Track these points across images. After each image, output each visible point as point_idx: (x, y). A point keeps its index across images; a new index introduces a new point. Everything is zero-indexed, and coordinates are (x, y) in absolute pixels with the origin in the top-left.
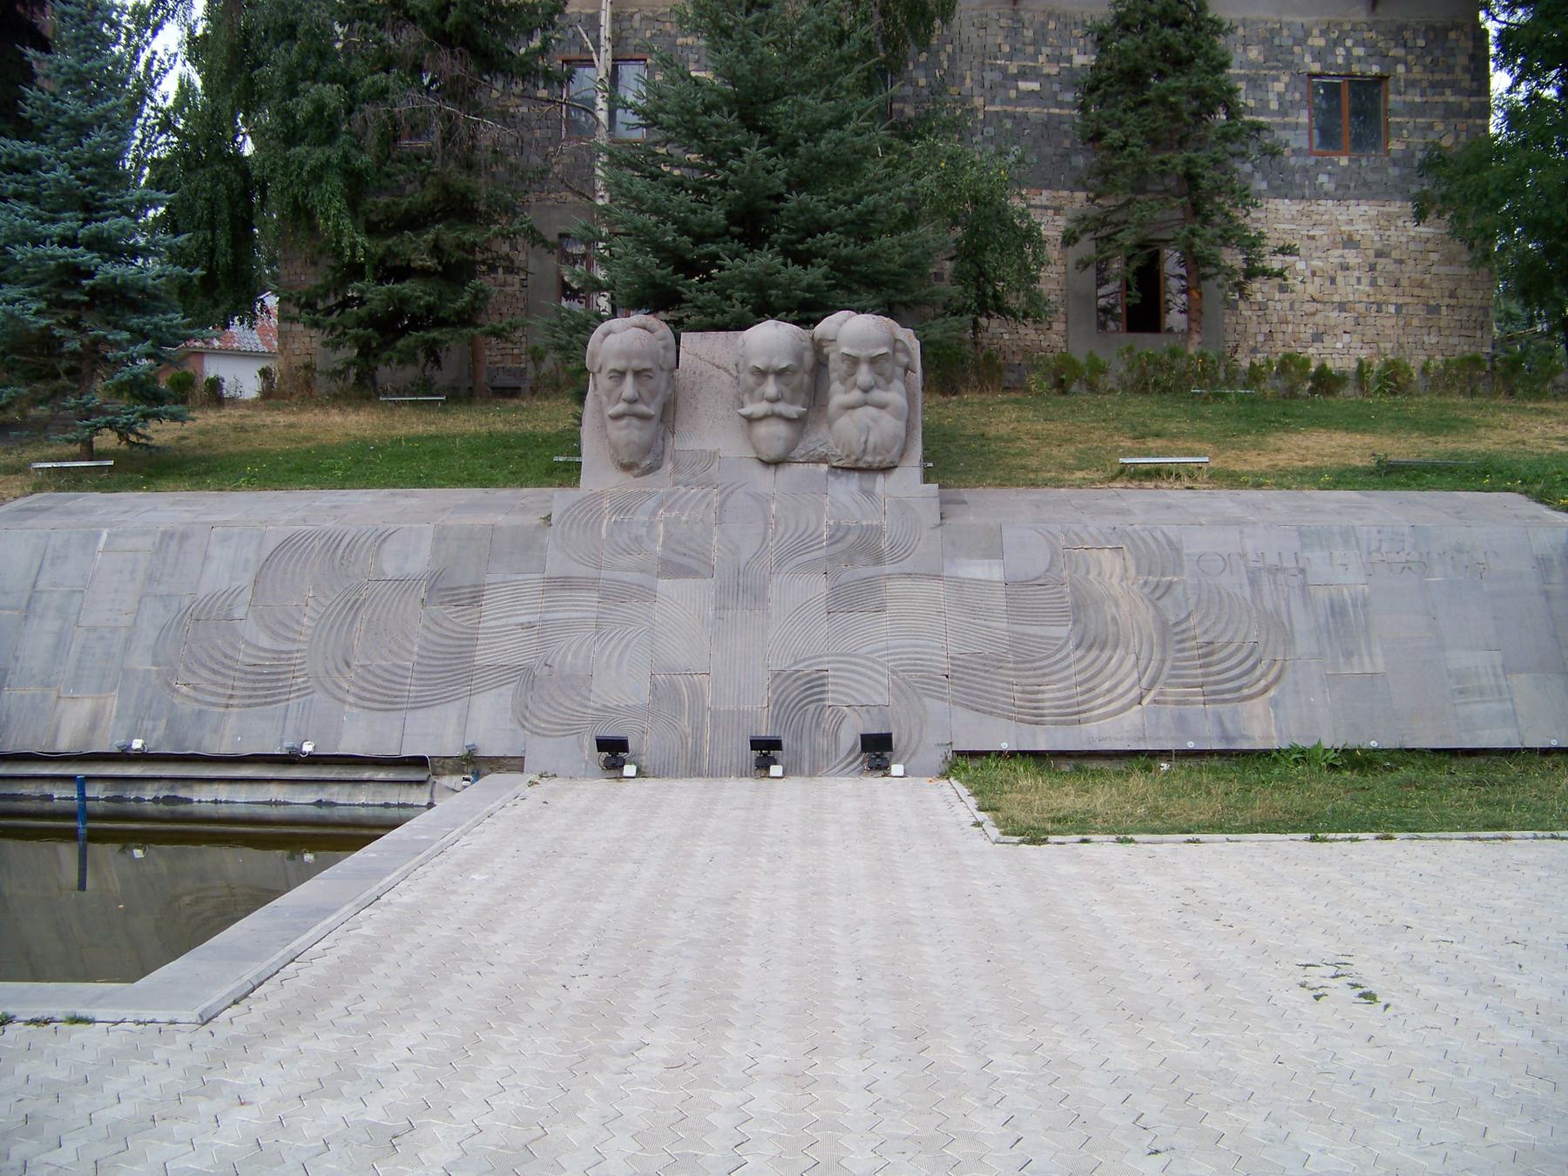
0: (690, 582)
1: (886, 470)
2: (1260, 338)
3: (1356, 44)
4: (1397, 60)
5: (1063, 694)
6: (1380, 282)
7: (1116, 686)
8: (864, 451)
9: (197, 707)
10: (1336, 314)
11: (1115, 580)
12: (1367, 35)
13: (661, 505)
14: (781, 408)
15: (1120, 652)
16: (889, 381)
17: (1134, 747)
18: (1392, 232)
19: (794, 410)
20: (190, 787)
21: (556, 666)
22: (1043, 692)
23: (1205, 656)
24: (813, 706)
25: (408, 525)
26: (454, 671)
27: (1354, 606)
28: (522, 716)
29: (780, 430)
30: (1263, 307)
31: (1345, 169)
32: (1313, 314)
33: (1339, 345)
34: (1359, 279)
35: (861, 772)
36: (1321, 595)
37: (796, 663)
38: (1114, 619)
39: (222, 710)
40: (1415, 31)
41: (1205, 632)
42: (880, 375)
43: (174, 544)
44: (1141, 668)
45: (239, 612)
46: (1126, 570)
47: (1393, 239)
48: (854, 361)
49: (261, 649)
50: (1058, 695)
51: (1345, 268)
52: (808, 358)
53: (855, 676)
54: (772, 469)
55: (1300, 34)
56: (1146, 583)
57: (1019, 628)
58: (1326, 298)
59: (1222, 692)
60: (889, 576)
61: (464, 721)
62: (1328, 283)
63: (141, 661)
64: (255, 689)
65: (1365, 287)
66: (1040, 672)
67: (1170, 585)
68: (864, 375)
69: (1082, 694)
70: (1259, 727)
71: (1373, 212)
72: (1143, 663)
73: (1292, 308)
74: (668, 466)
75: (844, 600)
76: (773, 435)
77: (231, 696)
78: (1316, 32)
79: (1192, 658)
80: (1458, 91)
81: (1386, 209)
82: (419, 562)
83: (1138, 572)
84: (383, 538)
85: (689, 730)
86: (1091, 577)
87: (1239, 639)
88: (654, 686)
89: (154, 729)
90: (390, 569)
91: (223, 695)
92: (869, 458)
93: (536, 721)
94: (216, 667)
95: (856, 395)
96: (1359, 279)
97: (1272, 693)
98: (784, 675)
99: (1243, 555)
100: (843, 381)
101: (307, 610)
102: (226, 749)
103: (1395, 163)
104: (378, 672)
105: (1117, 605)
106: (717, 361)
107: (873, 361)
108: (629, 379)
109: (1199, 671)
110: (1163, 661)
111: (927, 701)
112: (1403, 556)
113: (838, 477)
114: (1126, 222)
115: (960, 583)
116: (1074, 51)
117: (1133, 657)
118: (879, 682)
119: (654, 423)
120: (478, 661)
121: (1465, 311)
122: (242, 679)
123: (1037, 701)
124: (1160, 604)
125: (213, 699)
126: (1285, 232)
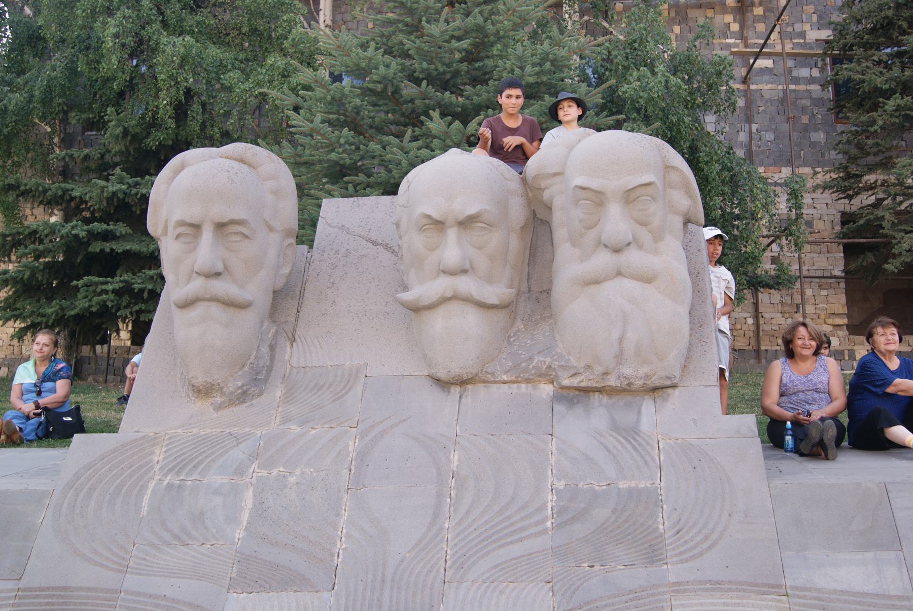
8: (620, 357)
13: (254, 456)
14: (466, 285)
16: (658, 237)
19: (494, 293)
29: (470, 322)
42: (643, 224)
48: (597, 199)
52: (517, 212)
54: (456, 390)
60: (678, 588)
76: (459, 335)
92: (627, 371)
95: (603, 260)
106: (374, 236)
107: (630, 196)
108: (207, 235)
116: (807, 27)
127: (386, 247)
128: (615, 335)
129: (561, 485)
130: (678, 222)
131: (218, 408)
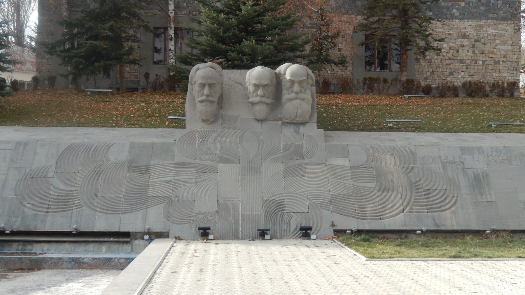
0: (231, 166)
1: (304, 124)
2: (429, 74)
5: (374, 208)
6: (476, 52)
7: (394, 206)
8: (296, 116)
10: (458, 64)
11: (392, 166)
13: (218, 136)
15: (395, 193)
16: (305, 90)
17: (402, 228)
18: (481, 32)
19: (269, 101)
20: (32, 245)
21: (180, 197)
22: (366, 208)
24: (280, 213)
25: (118, 141)
26: (140, 199)
27: (483, 176)
28: (168, 217)
30: (430, 62)
31: (463, 7)
32: (450, 64)
33: (460, 77)
34: (468, 51)
35: (300, 237)
36: (470, 172)
37: (273, 196)
38: (392, 180)
39: (45, 214)
41: (427, 186)
42: (302, 87)
44: (403, 199)
45: (50, 175)
46: (396, 162)
47: (482, 35)
49: (60, 189)
50: (372, 209)
51: (463, 46)
52: (274, 80)
53: (295, 201)
56: (403, 167)
57: (356, 184)
58: (455, 58)
59: (434, 208)
61: (145, 218)
62: (455, 52)
63: (9, 194)
64: (58, 205)
65: (470, 54)
66: (365, 200)
67: (413, 168)
68: (296, 88)
69: (381, 208)
70: (450, 221)
71: (474, 24)
72: (403, 197)
73: (441, 62)
74: (221, 121)
75: (290, 173)
76: (261, 110)
77: (48, 208)
79: (422, 195)
81: (479, 23)
82: (124, 156)
83: (400, 163)
84: (108, 147)
85: (233, 222)
86: (383, 164)
87: (440, 188)
88: (219, 205)
89: (16, 221)
90: (112, 159)
91: (45, 208)
92: (298, 119)
93: (173, 218)
94: (42, 197)
96: (468, 51)
97: (453, 209)
98: (269, 201)
99: (440, 157)
100: (288, 90)
101: (79, 174)
102: (47, 228)
103: (483, 5)
104: (109, 199)
105: (393, 175)
106: (237, 81)
107: (300, 82)
108: (207, 88)
109: (425, 200)
110: (411, 197)
111: (323, 211)
112: (501, 158)
113: (286, 126)
114: (378, 28)
115: (333, 167)
117: (400, 195)
118: (304, 204)
119: (215, 104)
120: (150, 195)
121: (510, 63)
122: (52, 202)
123: (364, 211)
124: (409, 175)
125: (41, 209)
126: (439, 32)
127: (241, 84)
128: (296, 112)
129: (284, 143)
130: (310, 86)
131: (208, 124)
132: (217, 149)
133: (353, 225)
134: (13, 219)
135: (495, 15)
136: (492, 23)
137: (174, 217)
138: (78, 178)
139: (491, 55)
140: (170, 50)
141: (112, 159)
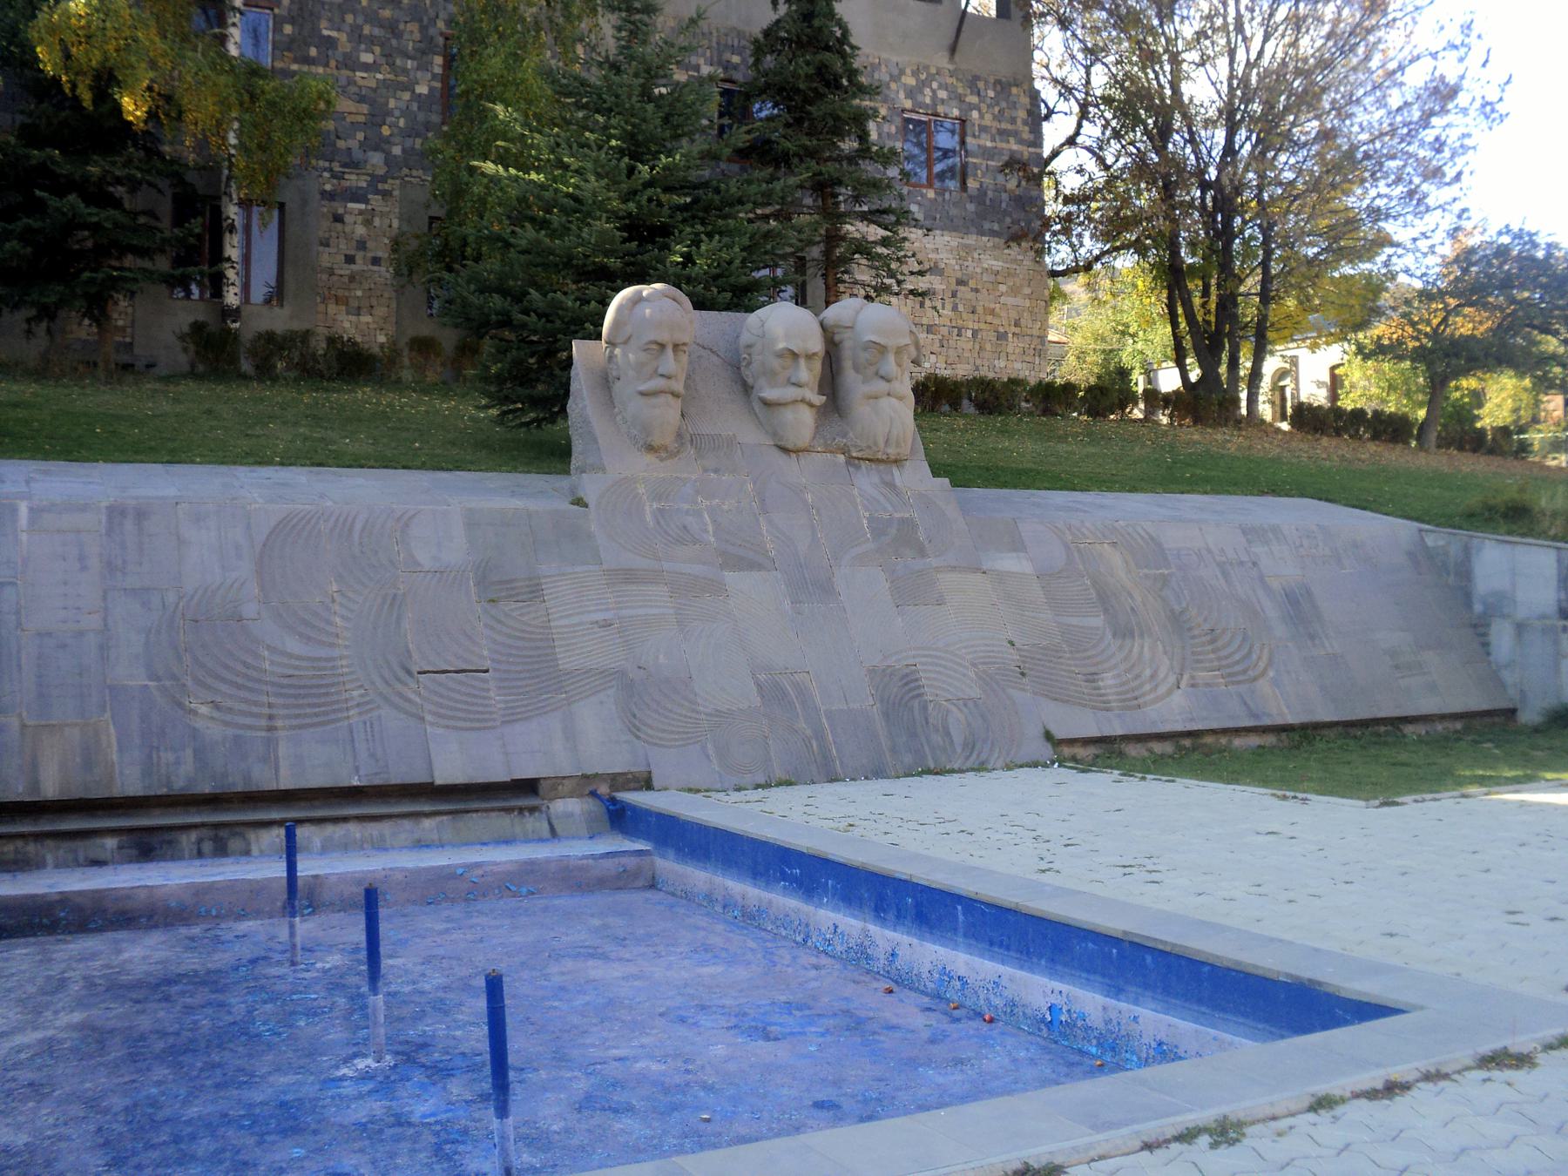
0: (756, 575)
3: (940, 87)
4: (972, 107)
6: (961, 308)
9: (230, 732)
12: (950, 80)
23: (1213, 641)
24: (916, 703)
40: (986, 82)
43: (129, 525)
45: (250, 610)
49: (291, 656)
55: (896, 72)
60: (938, 570)
65: (947, 312)
71: (954, 244)
76: (801, 423)
78: (908, 71)
80: (1021, 142)
81: (966, 241)
85: (809, 732)
89: (178, 763)
99: (1209, 551)
101: (337, 608)
102: (286, 782)
103: (971, 199)
111: (1011, 691)
113: (858, 468)
115: (1001, 577)
116: (702, 61)
125: (248, 721)
132: (706, 531)
133: (1089, 725)
134: (168, 757)
135: (996, 227)
136: (990, 244)
137: (651, 727)
138: (338, 620)
139: (989, 318)
140: (229, 259)
141: (424, 557)
